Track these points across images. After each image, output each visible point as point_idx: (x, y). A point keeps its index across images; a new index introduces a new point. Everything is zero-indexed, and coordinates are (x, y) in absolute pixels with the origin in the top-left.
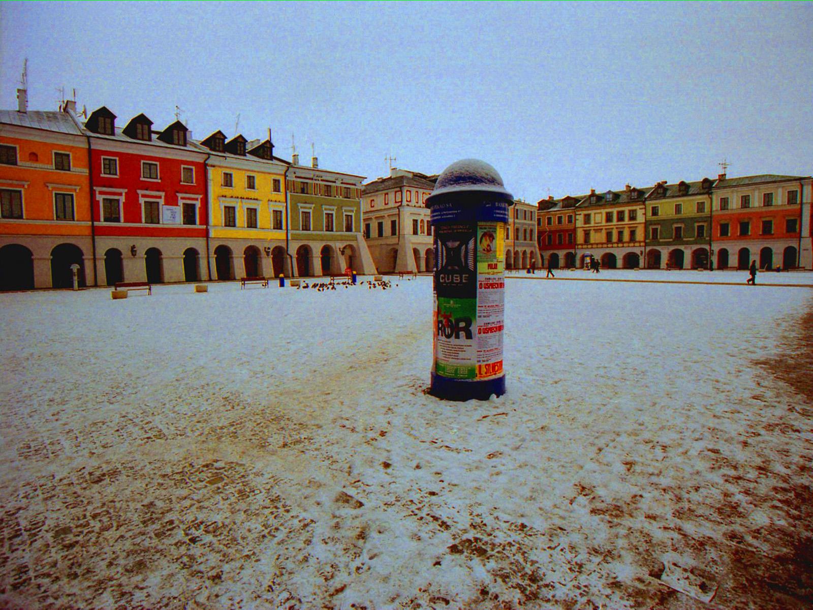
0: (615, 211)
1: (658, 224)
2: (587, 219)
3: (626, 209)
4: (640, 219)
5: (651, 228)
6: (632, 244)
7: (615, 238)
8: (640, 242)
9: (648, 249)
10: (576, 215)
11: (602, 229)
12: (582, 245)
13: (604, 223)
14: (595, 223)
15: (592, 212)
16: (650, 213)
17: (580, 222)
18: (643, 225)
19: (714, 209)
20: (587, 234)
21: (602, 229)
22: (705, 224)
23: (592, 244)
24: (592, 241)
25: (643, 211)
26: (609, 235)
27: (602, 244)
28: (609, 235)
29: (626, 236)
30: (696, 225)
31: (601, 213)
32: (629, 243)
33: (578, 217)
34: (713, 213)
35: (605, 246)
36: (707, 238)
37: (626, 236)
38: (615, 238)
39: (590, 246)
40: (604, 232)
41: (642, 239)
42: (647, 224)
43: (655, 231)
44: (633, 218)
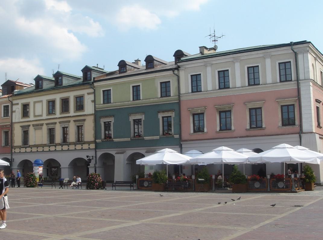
0: (57, 97)
1: (110, 116)
2: (25, 111)
3: (71, 95)
4: (89, 108)
5: (103, 121)
6: (79, 147)
7: (58, 138)
8: (89, 143)
9: (99, 153)
10: (12, 105)
11: (42, 125)
12: (20, 147)
13: (45, 116)
14: (35, 116)
15: (30, 100)
16: (101, 99)
17: (17, 116)
18: (92, 118)
19: (183, 91)
20: (26, 134)
21: (42, 125)
22: (172, 114)
23: (31, 147)
24: (31, 143)
25: (92, 97)
26: (51, 133)
27: (43, 146)
28: (51, 133)
29: (72, 137)
30: (160, 116)
31: (41, 101)
32: (75, 144)
33: (15, 108)
34: (182, 99)
35: (46, 149)
36: (177, 136)
37: (72, 137)
38: (58, 138)
39: (28, 150)
40: (45, 129)
41: (92, 139)
42: (98, 115)
43: (107, 126)
44: (80, 106)
